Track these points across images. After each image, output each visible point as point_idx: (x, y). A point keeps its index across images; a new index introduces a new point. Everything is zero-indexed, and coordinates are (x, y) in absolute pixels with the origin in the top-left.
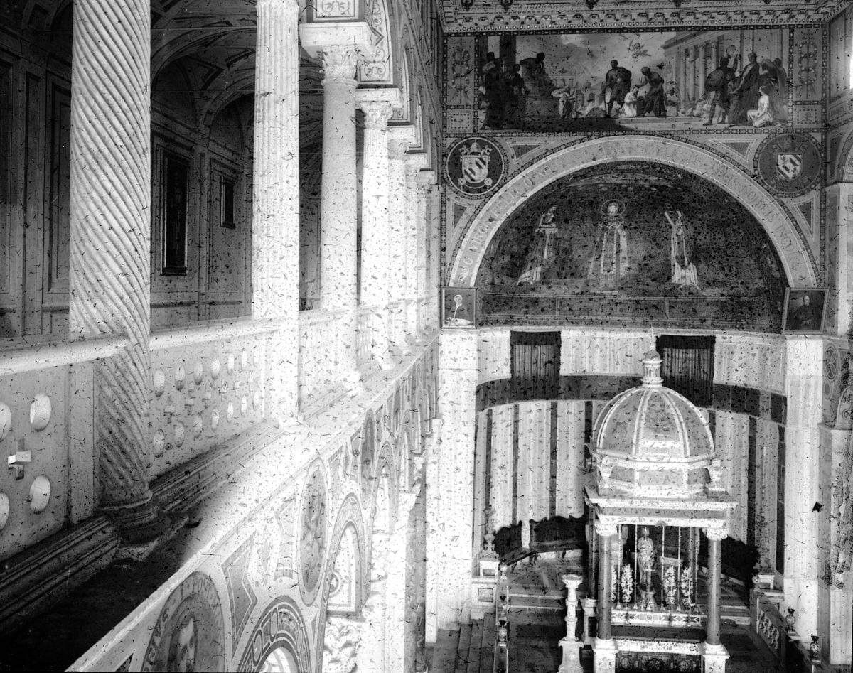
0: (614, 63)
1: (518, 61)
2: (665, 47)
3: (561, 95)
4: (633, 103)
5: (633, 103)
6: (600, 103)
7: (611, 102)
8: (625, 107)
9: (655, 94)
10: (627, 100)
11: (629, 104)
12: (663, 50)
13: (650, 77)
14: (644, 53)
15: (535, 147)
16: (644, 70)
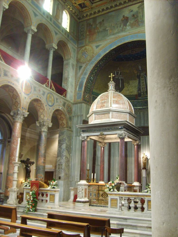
0: (124, 16)
1: (97, 23)
2: (138, 8)
3: (108, 29)
4: (129, 25)
5: (129, 25)
6: (120, 28)
7: (123, 26)
8: (127, 27)
9: (137, 20)
10: (128, 25)
11: (128, 26)
12: (138, 9)
13: (134, 17)
14: (132, 11)
15: (102, 44)
16: (132, 15)
